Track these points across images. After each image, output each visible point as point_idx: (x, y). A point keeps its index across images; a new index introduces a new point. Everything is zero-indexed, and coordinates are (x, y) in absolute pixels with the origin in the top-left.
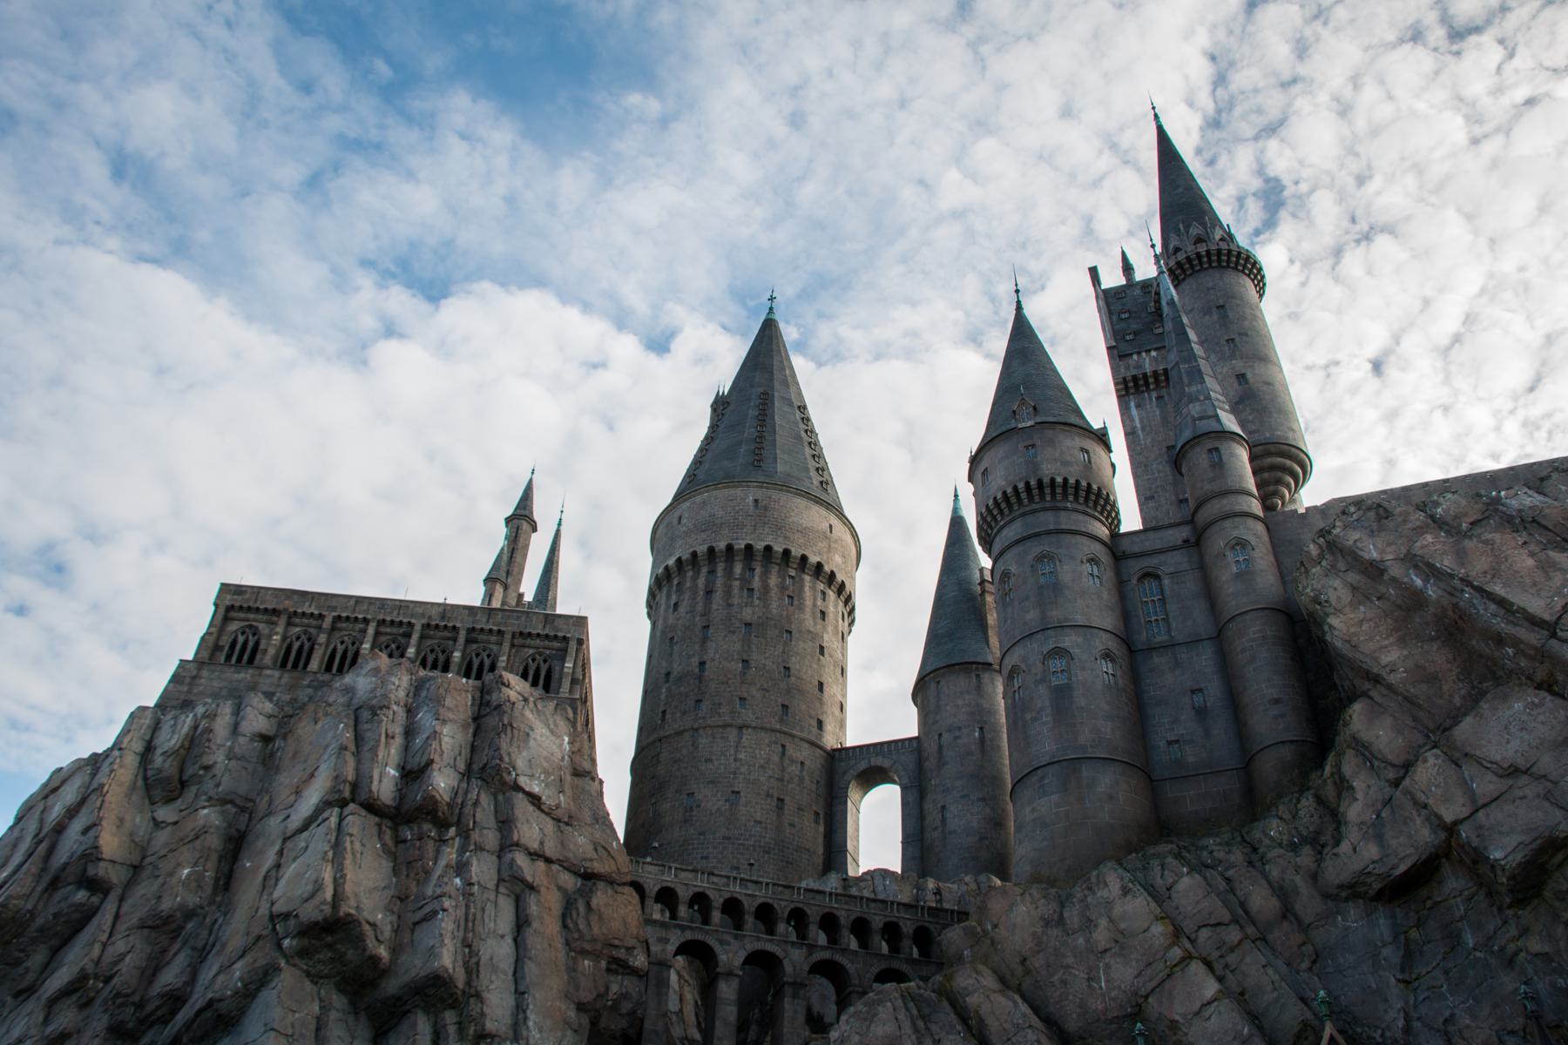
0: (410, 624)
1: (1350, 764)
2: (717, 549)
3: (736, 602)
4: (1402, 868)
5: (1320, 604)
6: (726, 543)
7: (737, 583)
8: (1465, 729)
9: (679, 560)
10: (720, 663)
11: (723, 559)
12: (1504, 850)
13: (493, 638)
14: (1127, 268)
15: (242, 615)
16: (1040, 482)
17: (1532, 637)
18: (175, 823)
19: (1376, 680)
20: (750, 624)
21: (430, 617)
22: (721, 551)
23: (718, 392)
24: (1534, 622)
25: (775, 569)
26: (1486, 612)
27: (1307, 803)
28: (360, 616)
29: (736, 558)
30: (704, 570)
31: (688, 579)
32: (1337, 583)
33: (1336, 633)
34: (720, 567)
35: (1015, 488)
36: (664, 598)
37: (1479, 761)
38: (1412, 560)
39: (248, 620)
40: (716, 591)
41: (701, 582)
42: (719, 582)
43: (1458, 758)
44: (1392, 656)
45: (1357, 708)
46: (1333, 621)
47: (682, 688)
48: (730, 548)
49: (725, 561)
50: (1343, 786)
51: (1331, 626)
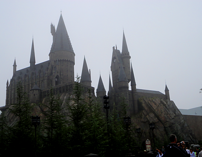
1: (143, 114)
8: (149, 114)
9: (63, 60)
12: (151, 122)
14: (116, 48)
17: (154, 110)
19: (145, 109)
24: (154, 109)
26: (152, 108)
27: (139, 115)
30: (66, 62)
34: (68, 62)
37: (150, 117)
38: (148, 103)
41: (66, 63)
43: (149, 116)
44: (146, 108)
45: (143, 111)
48: (69, 60)
50: (142, 115)
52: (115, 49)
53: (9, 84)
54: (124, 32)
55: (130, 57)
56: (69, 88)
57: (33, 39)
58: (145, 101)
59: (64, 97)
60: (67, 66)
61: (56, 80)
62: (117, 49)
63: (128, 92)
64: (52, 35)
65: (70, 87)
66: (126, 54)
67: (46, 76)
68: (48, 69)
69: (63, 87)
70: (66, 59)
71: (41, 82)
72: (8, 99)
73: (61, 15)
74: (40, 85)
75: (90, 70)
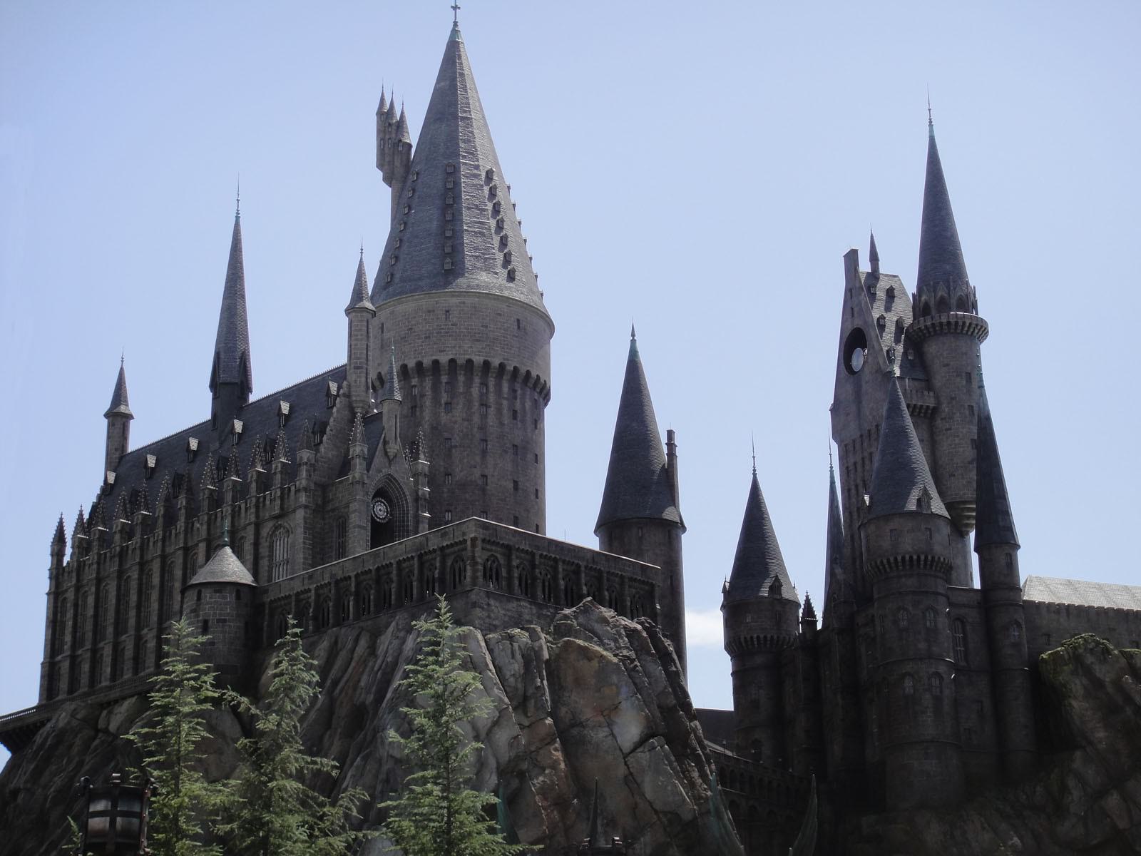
0: (578, 566)
1: (1071, 782)
2: (493, 365)
3: (506, 422)
4: (1095, 842)
5: (1066, 688)
6: (499, 362)
7: (505, 403)
9: (452, 361)
10: (499, 480)
11: (494, 375)
13: (617, 579)
14: (874, 258)
15: (488, 547)
16: (933, 558)
18: (528, 727)
20: (516, 446)
21: (587, 561)
22: (494, 368)
23: (382, 99)
25: (528, 392)
28: (553, 556)
29: (504, 377)
30: (477, 380)
31: (461, 384)
32: (1077, 682)
33: (1074, 710)
34: (492, 382)
35: (919, 557)
36: (429, 393)
39: (491, 550)
40: (490, 407)
41: (475, 391)
42: (492, 398)
44: (1101, 734)
45: (1078, 754)
46: (1074, 703)
47: (467, 496)
48: (502, 366)
49: (496, 378)
51: (1070, 704)
52: (865, 266)
53: (68, 551)
54: (931, 131)
55: (978, 330)
56: (442, 573)
57: (237, 218)
58: (1088, 672)
59: (404, 642)
60: (484, 404)
61: (381, 510)
62: (883, 269)
63: (942, 600)
64: (388, 180)
65: (449, 563)
66: (943, 305)
67: (304, 482)
68: (323, 432)
69: (399, 563)
70: (478, 360)
71: (270, 524)
72: (59, 658)
73: (455, 32)
74: (264, 551)
75: (670, 434)
